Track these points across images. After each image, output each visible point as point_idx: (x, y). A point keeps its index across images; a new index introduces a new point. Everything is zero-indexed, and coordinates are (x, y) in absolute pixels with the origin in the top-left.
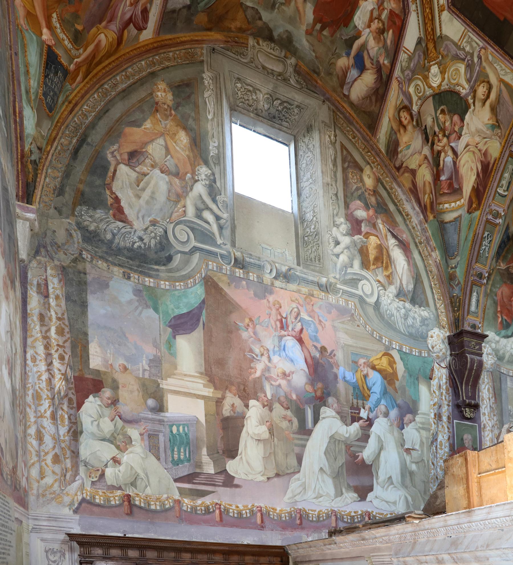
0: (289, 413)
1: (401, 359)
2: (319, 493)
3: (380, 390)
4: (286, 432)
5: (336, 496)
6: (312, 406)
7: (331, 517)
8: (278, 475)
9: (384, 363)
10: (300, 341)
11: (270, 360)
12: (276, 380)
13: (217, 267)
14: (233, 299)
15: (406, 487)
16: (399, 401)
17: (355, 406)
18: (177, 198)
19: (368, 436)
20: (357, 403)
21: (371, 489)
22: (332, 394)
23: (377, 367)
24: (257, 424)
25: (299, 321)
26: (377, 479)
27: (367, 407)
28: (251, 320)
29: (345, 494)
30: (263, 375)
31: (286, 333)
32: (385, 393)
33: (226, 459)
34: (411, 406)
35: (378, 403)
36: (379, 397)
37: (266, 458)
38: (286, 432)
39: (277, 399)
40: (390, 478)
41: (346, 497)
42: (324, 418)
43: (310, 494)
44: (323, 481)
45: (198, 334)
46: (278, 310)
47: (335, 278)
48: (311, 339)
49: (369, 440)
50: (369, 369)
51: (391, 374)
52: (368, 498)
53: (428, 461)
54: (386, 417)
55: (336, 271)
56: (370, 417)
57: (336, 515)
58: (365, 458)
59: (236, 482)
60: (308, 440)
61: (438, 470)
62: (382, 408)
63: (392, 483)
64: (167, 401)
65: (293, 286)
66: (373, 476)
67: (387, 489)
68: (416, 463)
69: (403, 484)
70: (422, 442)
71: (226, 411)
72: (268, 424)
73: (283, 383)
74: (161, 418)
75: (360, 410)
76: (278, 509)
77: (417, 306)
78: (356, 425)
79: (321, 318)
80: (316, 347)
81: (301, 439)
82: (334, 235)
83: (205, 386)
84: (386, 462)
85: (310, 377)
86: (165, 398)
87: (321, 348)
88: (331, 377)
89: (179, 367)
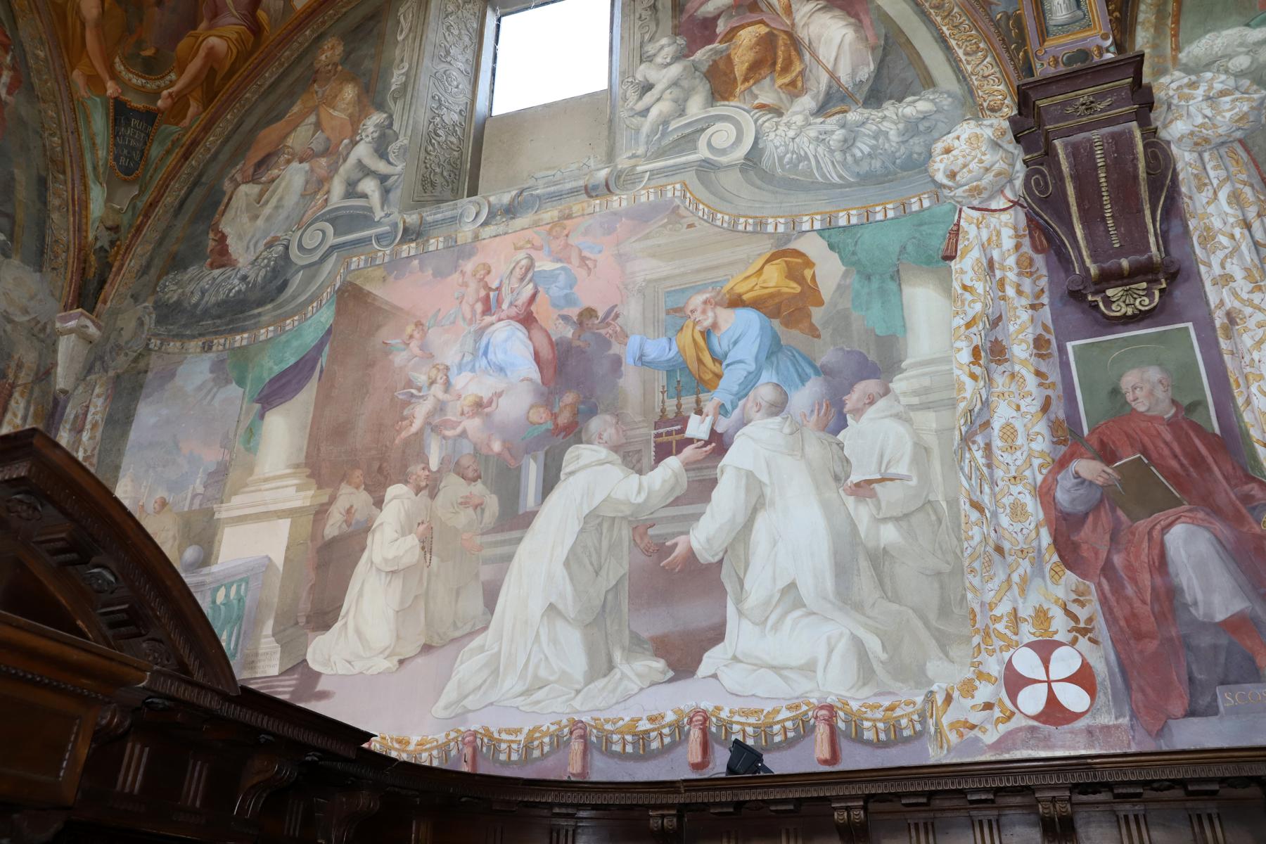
0: (478, 488)
1: (832, 247)
2: (536, 677)
3: (755, 349)
6: (541, 455)
7: (568, 743)
8: (427, 648)
9: (774, 277)
10: (527, 320)
11: (448, 385)
12: (454, 425)
13: (366, 261)
14: (387, 303)
15: (858, 607)
16: (827, 355)
17: (671, 416)
18: (319, 184)
19: (714, 482)
20: (679, 406)
21: (717, 635)
22: (601, 407)
23: (745, 297)
24: (396, 535)
25: (530, 281)
26: (739, 601)
27: (709, 407)
28: (419, 324)
30: (427, 423)
31: (494, 318)
32: (773, 350)
33: (311, 635)
34: (872, 357)
36: (752, 367)
37: (403, 613)
39: (452, 466)
40: (792, 586)
41: (624, 675)
42: (572, 473)
43: (510, 684)
45: (307, 396)
46: (481, 280)
47: (634, 156)
48: (555, 305)
49: (715, 494)
50: (719, 310)
51: (795, 296)
52: (704, 669)
53: (953, 503)
54: (777, 414)
55: (637, 143)
56: (719, 430)
58: (696, 546)
59: (320, 687)
60: (520, 540)
61: (1005, 520)
62: (765, 392)
63: (799, 603)
64: (220, 542)
65: (520, 222)
66: (724, 592)
67: (775, 628)
68: (899, 520)
69: (846, 598)
70: (921, 452)
71: (333, 527)
72: (422, 528)
73: (473, 425)
74: (201, 579)
75: (684, 421)
76: (415, 739)
77: (885, 105)
78: (673, 462)
79: (586, 253)
80: (566, 318)
81: (503, 543)
82: (639, 77)
83: (299, 488)
84: (774, 544)
85: (544, 389)
86: (217, 538)
87: (581, 315)
89: (257, 470)
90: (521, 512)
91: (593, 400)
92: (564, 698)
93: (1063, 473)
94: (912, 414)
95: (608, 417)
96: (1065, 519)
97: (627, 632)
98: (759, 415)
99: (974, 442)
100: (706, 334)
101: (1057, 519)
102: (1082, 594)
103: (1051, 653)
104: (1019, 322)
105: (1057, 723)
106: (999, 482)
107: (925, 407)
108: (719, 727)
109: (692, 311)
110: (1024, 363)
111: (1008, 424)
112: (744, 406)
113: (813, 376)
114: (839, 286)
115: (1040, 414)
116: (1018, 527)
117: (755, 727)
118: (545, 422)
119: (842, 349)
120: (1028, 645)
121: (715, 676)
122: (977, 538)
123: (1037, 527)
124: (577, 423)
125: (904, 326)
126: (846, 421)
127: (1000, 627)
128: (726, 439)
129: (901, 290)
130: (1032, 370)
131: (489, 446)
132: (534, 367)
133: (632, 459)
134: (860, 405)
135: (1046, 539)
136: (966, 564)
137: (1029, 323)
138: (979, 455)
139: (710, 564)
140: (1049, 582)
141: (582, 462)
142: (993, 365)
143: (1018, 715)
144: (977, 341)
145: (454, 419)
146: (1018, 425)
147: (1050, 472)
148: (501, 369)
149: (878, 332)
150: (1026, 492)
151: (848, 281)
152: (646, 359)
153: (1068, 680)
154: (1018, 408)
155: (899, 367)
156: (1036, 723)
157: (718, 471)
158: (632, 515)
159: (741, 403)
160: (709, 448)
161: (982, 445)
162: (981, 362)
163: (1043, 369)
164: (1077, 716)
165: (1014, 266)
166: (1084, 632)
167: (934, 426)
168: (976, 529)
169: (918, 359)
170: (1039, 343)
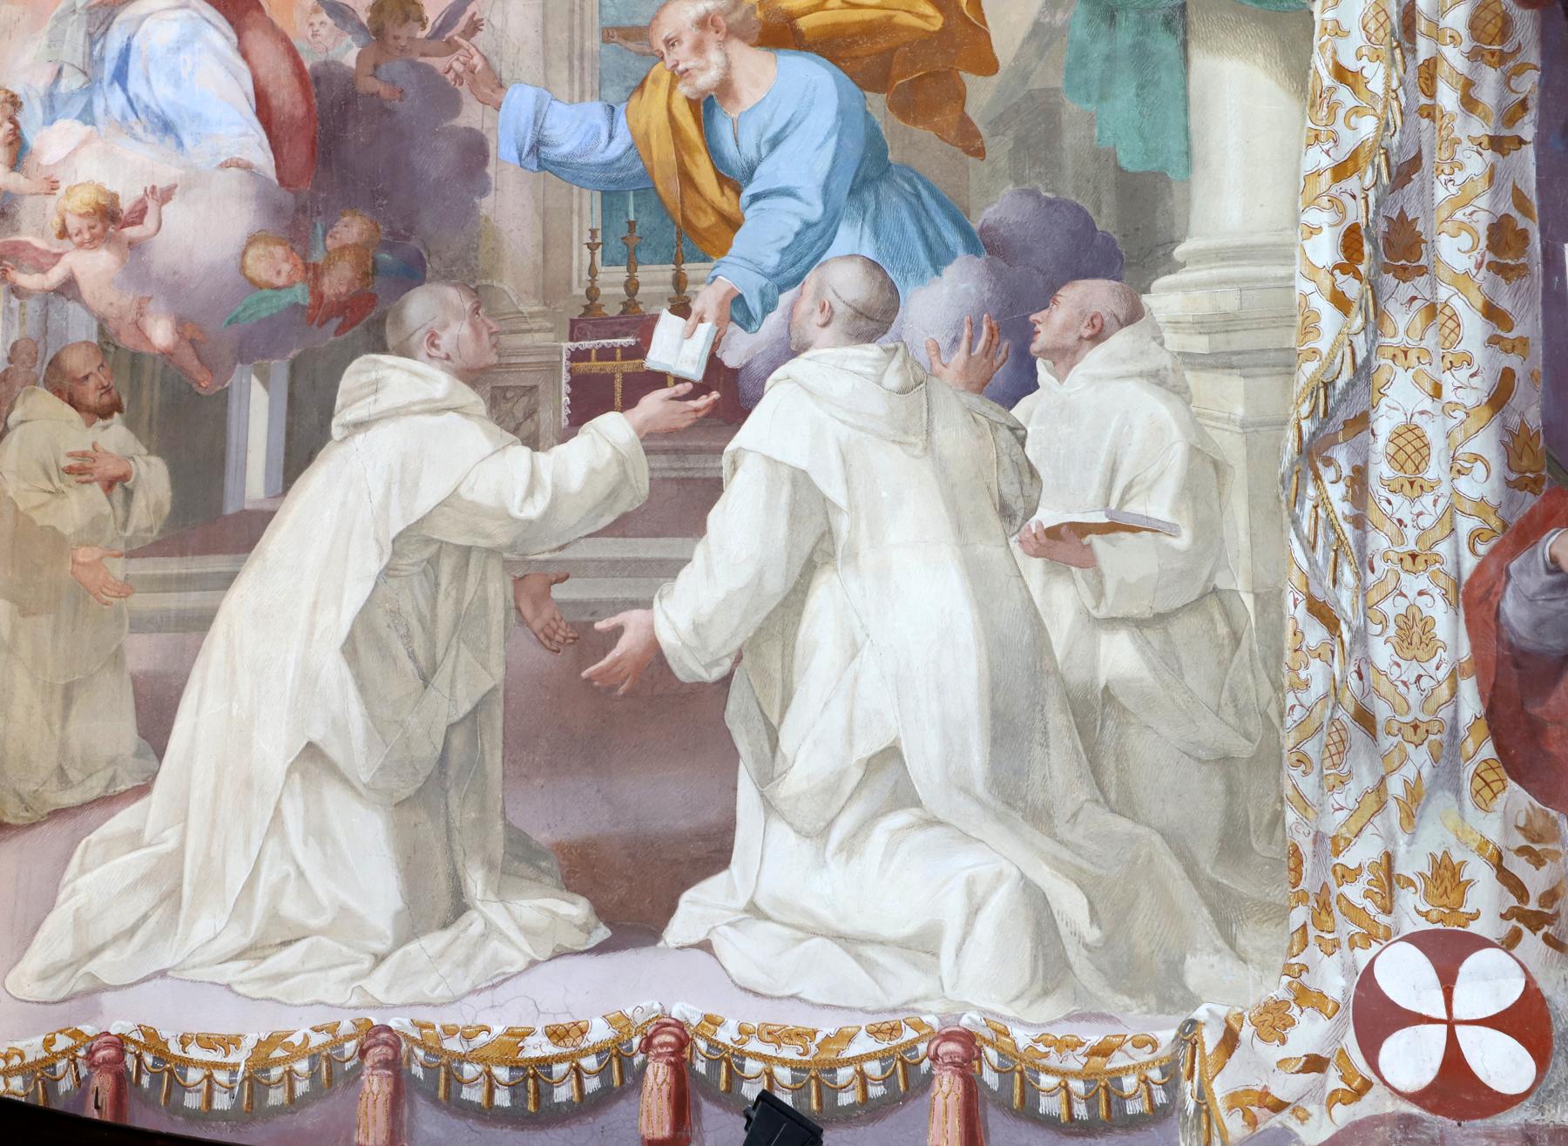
0: (114, 436)
2: (274, 917)
3: (823, 164)
4: (84, 555)
5: (412, 925)
6: (280, 368)
12: (43, 262)
15: (1041, 818)
16: (999, 205)
17: (612, 310)
19: (714, 489)
20: (631, 286)
21: (711, 852)
22: (433, 264)
23: (804, 23)
26: (766, 778)
27: (706, 300)
29: (487, 907)
32: (867, 174)
34: (1105, 223)
35: (807, 251)
36: (816, 212)
38: (84, 555)
39: (41, 369)
40: (892, 754)
41: (490, 930)
42: (360, 425)
43: (209, 929)
44: (319, 833)
49: (715, 517)
50: (738, 49)
51: (927, 38)
52: (679, 930)
53: (1269, 600)
54: (869, 338)
56: (731, 359)
57: (395, 1065)
58: (667, 638)
60: (228, 580)
61: (1382, 653)
62: (842, 279)
63: (904, 796)
66: (733, 756)
67: (851, 846)
69: (1013, 795)
73: (95, 267)
75: (645, 328)
81: (184, 583)
84: (854, 651)
88: (436, 162)
90: (230, 509)
91: (414, 243)
92: (345, 971)
93: (1524, 556)
94: (1190, 377)
95: (452, 294)
96: (1517, 665)
97: (499, 827)
98: (827, 331)
99: (1328, 462)
100: (705, 108)
101: (1499, 662)
102: (1539, 838)
103: (1460, 961)
104: (1459, 177)
105: (1462, 1113)
106: (1379, 564)
107: (1222, 362)
108: (713, 1064)
109: (670, 43)
110: (1461, 281)
111: (1411, 428)
112: (793, 307)
113: (961, 252)
114: (1037, 30)
115: (1486, 413)
116: (1410, 671)
117: (797, 1068)
118: (290, 285)
119: (1034, 193)
120: (1412, 939)
121: (706, 946)
122: (1318, 687)
123: (1453, 676)
124: (372, 299)
125: (1188, 153)
126: (1034, 374)
127: (1354, 892)
128: (746, 386)
129: (1186, 60)
130: (1479, 303)
131: (138, 327)
132: (257, 134)
133: (512, 405)
134: (1070, 339)
135: (1470, 705)
136: (1289, 743)
137: (1482, 184)
138: (1336, 493)
139: (702, 685)
140: (1468, 803)
141: (386, 401)
142: (1389, 280)
143: (1377, 1088)
144: (1356, 213)
145: (39, 243)
146: (1433, 431)
147: (1493, 551)
148: (167, 127)
149: (1124, 162)
150: (1436, 592)
151: (1060, 18)
152: (552, 153)
153: (1492, 1022)
154: (1437, 392)
155: (1168, 256)
156: (1415, 1110)
157: (725, 460)
158: (512, 547)
159: (785, 299)
160: (703, 401)
161: (1346, 471)
162: (1362, 268)
163: (1505, 303)
164: (1506, 1102)
165: (1464, 32)
166: (1535, 921)
167: (1239, 411)
168: (1316, 665)
169: (1215, 242)
170: (1502, 236)
